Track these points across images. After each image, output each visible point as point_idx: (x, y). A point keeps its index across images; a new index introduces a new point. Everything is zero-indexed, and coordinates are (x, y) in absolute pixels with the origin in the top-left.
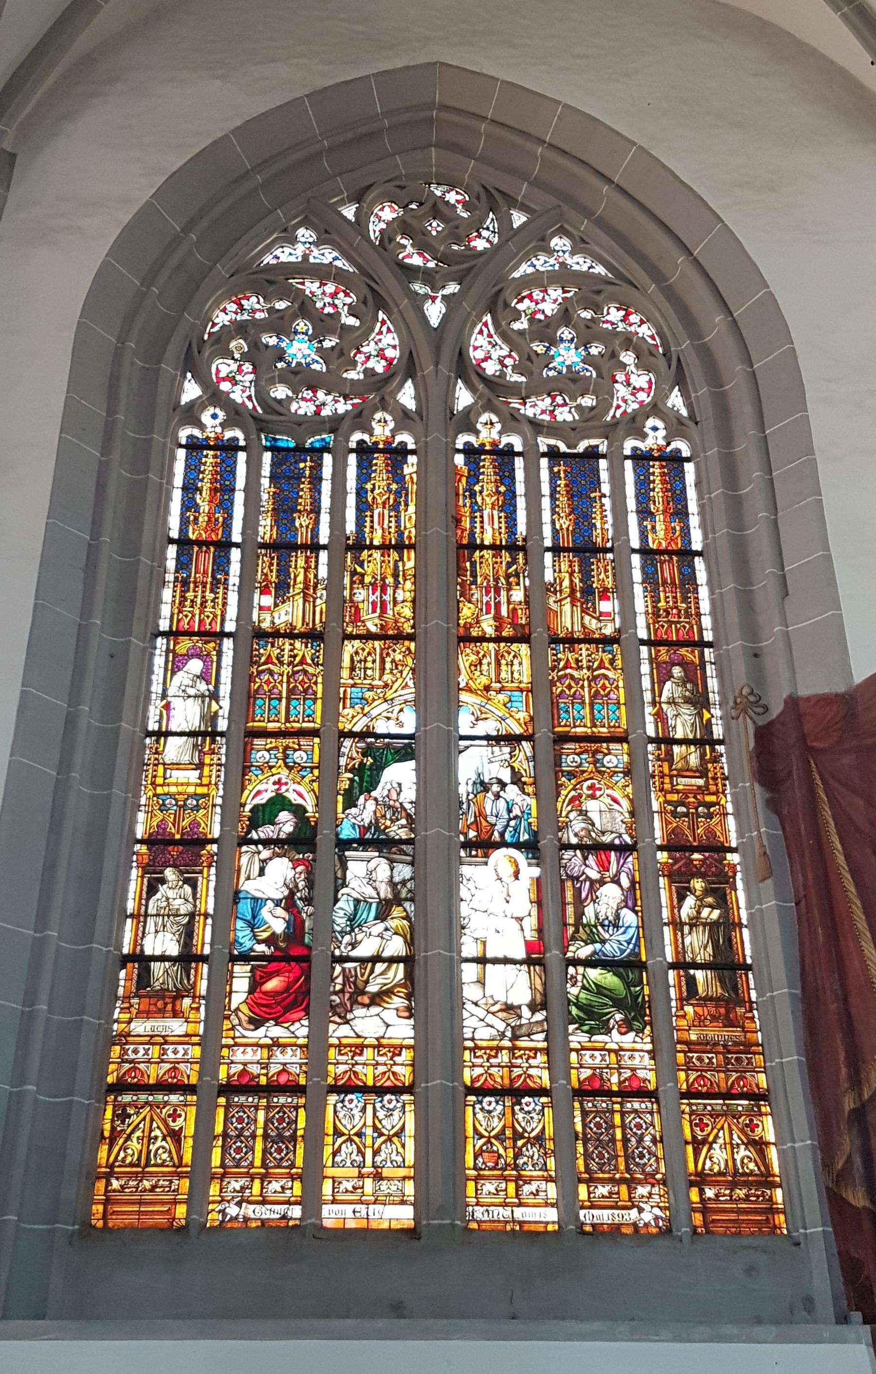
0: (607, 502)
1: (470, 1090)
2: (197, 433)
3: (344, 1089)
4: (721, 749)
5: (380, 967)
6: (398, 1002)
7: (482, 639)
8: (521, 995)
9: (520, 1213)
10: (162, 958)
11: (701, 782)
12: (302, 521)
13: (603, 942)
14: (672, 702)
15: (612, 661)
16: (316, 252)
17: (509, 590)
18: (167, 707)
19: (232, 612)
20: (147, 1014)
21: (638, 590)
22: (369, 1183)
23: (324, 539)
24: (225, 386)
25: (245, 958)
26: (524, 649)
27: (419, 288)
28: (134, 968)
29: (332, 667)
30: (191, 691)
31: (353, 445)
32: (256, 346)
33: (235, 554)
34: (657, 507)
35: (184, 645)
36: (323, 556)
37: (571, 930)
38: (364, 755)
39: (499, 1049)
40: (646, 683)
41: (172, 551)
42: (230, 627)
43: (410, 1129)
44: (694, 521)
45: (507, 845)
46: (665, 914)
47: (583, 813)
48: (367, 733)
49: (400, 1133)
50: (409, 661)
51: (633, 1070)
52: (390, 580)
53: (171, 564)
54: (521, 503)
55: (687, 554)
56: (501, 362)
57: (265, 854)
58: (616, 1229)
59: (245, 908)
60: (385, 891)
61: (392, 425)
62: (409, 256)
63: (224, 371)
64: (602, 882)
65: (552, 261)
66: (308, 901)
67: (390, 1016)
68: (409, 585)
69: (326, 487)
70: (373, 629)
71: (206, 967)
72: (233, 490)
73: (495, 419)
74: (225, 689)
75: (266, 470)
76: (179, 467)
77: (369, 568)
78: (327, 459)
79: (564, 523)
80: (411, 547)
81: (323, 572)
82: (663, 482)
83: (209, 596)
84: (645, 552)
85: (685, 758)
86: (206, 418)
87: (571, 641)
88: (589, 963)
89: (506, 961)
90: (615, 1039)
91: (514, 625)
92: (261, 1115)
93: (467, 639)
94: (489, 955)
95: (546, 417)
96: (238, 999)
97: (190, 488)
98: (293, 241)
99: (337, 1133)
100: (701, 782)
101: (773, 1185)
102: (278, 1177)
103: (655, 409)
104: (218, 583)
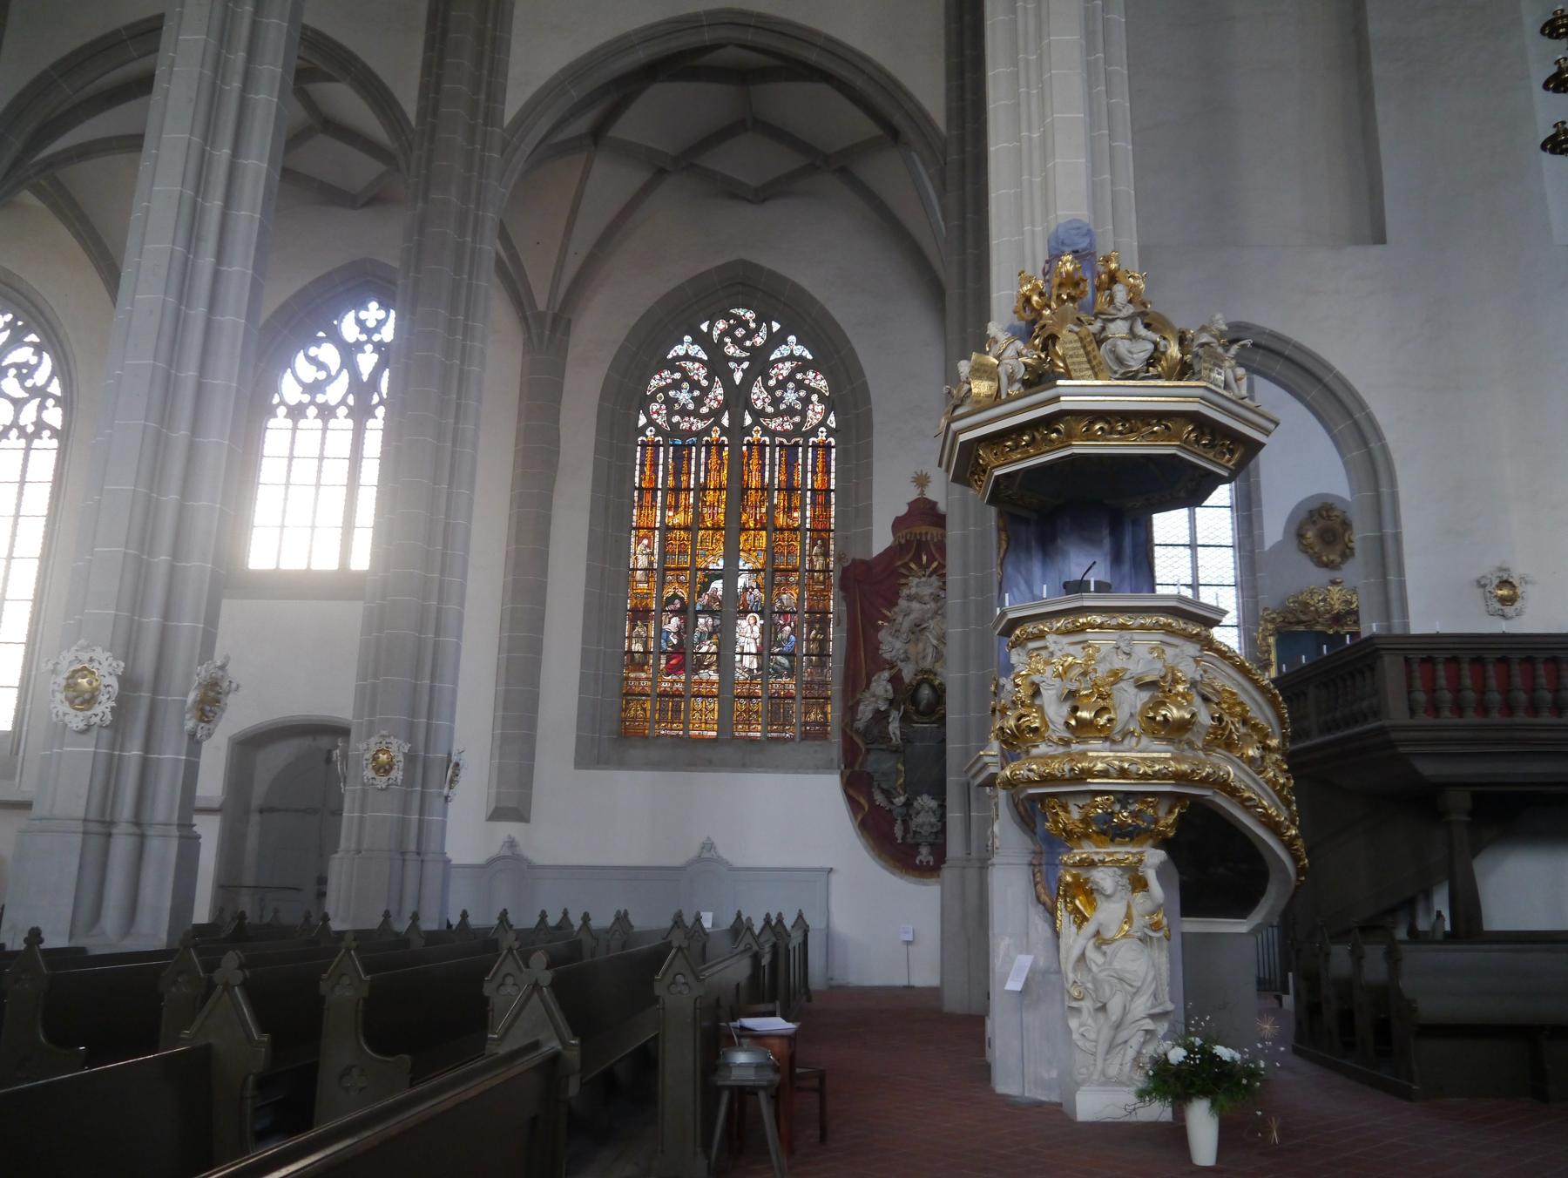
0: (800, 467)
1: (736, 697)
2: (644, 439)
3: (696, 696)
4: (831, 573)
5: (708, 656)
6: (714, 668)
7: (749, 529)
8: (755, 666)
9: (750, 734)
10: (638, 652)
11: (823, 587)
12: (684, 478)
13: (783, 647)
14: (816, 555)
15: (796, 538)
16: (691, 347)
17: (760, 507)
18: (636, 558)
19: (658, 519)
20: (634, 671)
21: (808, 507)
22: (703, 725)
23: (692, 487)
24: (655, 416)
25: (664, 652)
26: (764, 533)
27: (732, 365)
28: (629, 655)
29: (694, 542)
30: (644, 552)
31: (704, 443)
32: (666, 396)
33: (659, 493)
34: (819, 469)
35: (642, 532)
36: (692, 493)
37: (772, 643)
38: (705, 577)
39: (746, 683)
40: (807, 547)
41: (636, 493)
42: (658, 525)
43: (716, 708)
44: (833, 475)
45: (753, 612)
46: (805, 636)
47: (781, 600)
48: (706, 569)
49: (714, 709)
50: (722, 539)
51: (789, 690)
52: (716, 504)
53: (636, 499)
54: (767, 468)
55: (829, 491)
56: (763, 400)
57: (671, 616)
58: (777, 739)
59: (664, 635)
60: (710, 628)
61: (719, 432)
62: (729, 348)
63: (655, 408)
64: (785, 625)
65: (788, 348)
66: (685, 633)
67: (711, 673)
68: (723, 506)
69: (693, 462)
70: (709, 525)
71: (651, 656)
72: (658, 465)
73: (759, 429)
74: (656, 551)
75: (671, 456)
76: (638, 455)
77: (708, 498)
78: (694, 449)
79: (783, 477)
80: (724, 489)
81: (691, 500)
82: (823, 458)
83: (650, 512)
84: (813, 490)
85: (818, 578)
86: (648, 433)
87: (782, 530)
88: (777, 654)
89: (750, 654)
90: (784, 680)
91: (761, 523)
92: (670, 704)
93: (744, 529)
94: (745, 651)
95: (779, 428)
96: (662, 666)
97: (642, 465)
98: (682, 343)
99: (694, 710)
100: (823, 587)
101: (828, 726)
102: (676, 723)
103: (823, 423)
104: (653, 506)
